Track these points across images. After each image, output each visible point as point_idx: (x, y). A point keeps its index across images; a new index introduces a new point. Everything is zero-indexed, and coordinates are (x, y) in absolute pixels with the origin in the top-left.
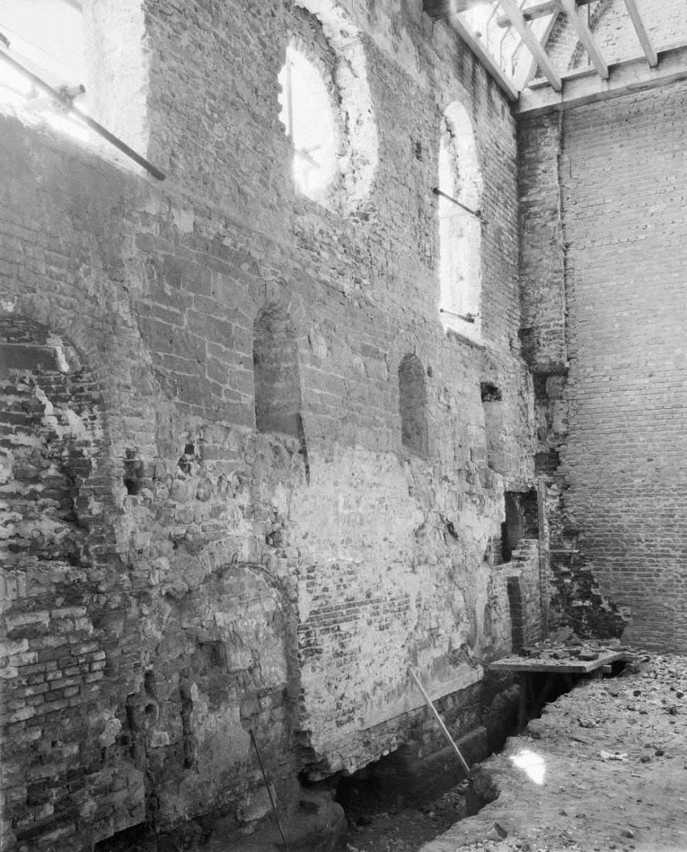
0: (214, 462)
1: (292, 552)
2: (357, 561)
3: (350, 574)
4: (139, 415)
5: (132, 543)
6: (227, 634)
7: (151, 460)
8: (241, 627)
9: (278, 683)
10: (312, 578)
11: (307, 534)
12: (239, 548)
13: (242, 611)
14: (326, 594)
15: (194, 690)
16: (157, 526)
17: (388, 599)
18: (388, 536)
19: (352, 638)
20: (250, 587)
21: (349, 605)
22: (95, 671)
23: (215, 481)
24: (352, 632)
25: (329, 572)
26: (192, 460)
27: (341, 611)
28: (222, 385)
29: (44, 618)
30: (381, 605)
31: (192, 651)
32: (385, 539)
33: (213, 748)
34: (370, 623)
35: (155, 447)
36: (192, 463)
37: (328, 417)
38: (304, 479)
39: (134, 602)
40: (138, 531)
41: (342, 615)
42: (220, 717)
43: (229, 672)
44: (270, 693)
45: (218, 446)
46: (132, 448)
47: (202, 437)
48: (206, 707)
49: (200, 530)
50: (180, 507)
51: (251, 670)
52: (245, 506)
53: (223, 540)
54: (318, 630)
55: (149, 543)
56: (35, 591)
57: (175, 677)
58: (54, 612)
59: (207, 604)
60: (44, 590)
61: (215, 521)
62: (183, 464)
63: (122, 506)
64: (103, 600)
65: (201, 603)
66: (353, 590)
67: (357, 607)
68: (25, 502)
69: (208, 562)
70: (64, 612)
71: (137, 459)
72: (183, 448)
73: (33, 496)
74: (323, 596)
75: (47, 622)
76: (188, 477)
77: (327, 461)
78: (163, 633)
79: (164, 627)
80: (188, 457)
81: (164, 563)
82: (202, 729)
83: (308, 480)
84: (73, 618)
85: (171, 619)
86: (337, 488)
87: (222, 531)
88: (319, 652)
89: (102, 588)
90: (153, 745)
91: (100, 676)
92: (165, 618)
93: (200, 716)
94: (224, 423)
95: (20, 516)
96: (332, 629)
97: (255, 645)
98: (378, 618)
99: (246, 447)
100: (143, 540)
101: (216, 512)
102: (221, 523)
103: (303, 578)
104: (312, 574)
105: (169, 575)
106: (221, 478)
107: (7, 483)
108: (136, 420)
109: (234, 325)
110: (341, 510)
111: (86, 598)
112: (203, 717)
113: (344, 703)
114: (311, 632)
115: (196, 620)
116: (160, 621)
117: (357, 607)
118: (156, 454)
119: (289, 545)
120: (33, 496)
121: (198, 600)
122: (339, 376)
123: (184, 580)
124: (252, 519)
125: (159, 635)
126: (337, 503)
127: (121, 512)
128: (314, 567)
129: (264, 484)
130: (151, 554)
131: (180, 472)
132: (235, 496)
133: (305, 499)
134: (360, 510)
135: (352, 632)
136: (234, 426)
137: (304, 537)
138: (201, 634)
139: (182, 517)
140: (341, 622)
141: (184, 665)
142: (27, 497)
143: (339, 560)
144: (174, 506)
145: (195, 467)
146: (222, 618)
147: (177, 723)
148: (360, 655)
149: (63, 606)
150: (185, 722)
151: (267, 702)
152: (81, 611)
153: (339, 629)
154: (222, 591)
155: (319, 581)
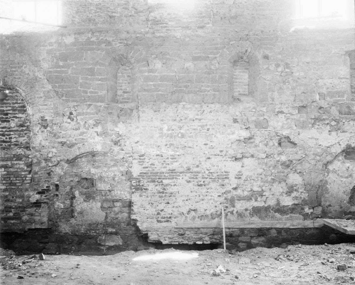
0: (82, 117)
1: (128, 149)
2: (178, 153)
3: (172, 159)
4: (46, 105)
5: (40, 144)
6: (96, 176)
7: (51, 118)
8: (104, 174)
9: (125, 198)
10: (142, 159)
11: (138, 142)
12: (95, 146)
13: (105, 169)
14: (153, 166)
15: (77, 193)
16: (53, 139)
17: (207, 172)
18: (208, 142)
19: (172, 187)
20: (111, 160)
21: (172, 172)
22: (27, 180)
23: (82, 123)
24: (173, 184)
25: (155, 157)
26: (74, 117)
27: (165, 174)
28: (88, 90)
29: (9, 163)
30: (200, 175)
31: (77, 180)
32: (206, 144)
33: (84, 214)
34: (189, 182)
35: (53, 114)
36: (74, 118)
37: (160, 93)
38: (137, 120)
39: (43, 161)
40: (43, 140)
41: (165, 176)
42: (89, 204)
43: (97, 190)
44: (120, 201)
45: (85, 111)
46: (42, 115)
47: (76, 109)
48: (82, 199)
49: (74, 140)
50: (63, 132)
51: (110, 191)
52: (99, 131)
53: (86, 144)
54: (145, 181)
55: (47, 144)
56: (7, 156)
57: (68, 188)
58: (13, 162)
59: (86, 165)
60: (9, 156)
61: (81, 137)
62: (69, 118)
63: (36, 133)
64: (30, 160)
65: (83, 165)
66: (175, 165)
67: (178, 174)
68: (19, 132)
69: (77, 150)
70: (15, 162)
71: (45, 119)
72: (68, 114)
73: (22, 130)
74: (151, 167)
75: (10, 164)
76: (72, 122)
77: (155, 111)
78: (64, 172)
79: (64, 171)
80: (72, 116)
81: (54, 150)
82: (79, 207)
83: (139, 120)
84: (19, 164)
85: (67, 169)
86: (162, 122)
87: (85, 140)
88: (146, 189)
89: (30, 157)
90: (56, 206)
91: (29, 181)
92: (65, 168)
93: (79, 202)
94: (88, 103)
95: (18, 136)
96: (157, 181)
97: (112, 182)
98: (196, 180)
99: (101, 110)
100: (43, 143)
101: (82, 134)
102: (85, 138)
103: (135, 159)
104: (142, 158)
105: (57, 154)
106: (86, 122)
107: (14, 128)
108: (45, 107)
109: (96, 68)
110: (165, 131)
111: (24, 159)
112: (80, 203)
113: (162, 213)
114: (141, 181)
115: (80, 170)
116: (62, 169)
117: (178, 174)
118: (53, 116)
119: (125, 145)
120: (22, 130)
121: (81, 163)
122: (171, 74)
123: (65, 156)
124: (103, 136)
125: (62, 174)
126: (161, 129)
127: (37, 135)
128: (144, 155)
129: (110, 123)
130: (48, 148)
131: (69, 121)
132: (93, 128)
133: (138, 127)
134: (182, 131)
135: (173, 184)
136: (94, 103)
137: (136, 143)
138: (82, 175)
139: (64, 136)
140: (164, 179)
141: (72, 184)
142: (20, 131)
143: (163, 153)
144: (61, 132)
145: (75, 119)
146: (93, 171)
147: (68, 202)
148: (177, 195)
149: (15, 160)
150: (72, 204)
151: (118, 204)
152: (21, 162)
153: (162, 182)
154: (95, 161)
155: (147, 160)
